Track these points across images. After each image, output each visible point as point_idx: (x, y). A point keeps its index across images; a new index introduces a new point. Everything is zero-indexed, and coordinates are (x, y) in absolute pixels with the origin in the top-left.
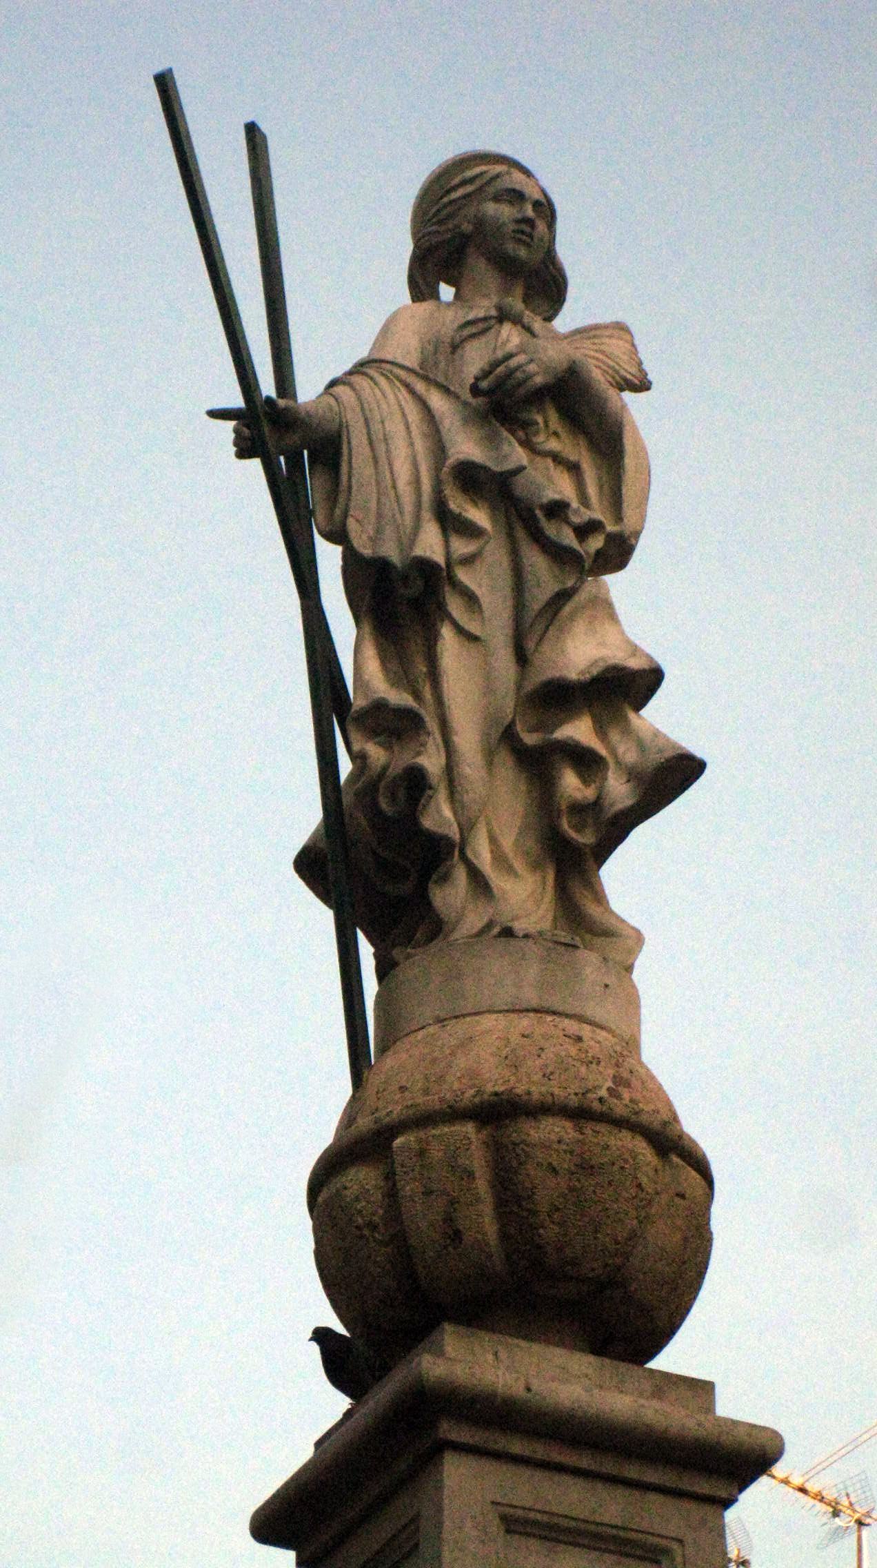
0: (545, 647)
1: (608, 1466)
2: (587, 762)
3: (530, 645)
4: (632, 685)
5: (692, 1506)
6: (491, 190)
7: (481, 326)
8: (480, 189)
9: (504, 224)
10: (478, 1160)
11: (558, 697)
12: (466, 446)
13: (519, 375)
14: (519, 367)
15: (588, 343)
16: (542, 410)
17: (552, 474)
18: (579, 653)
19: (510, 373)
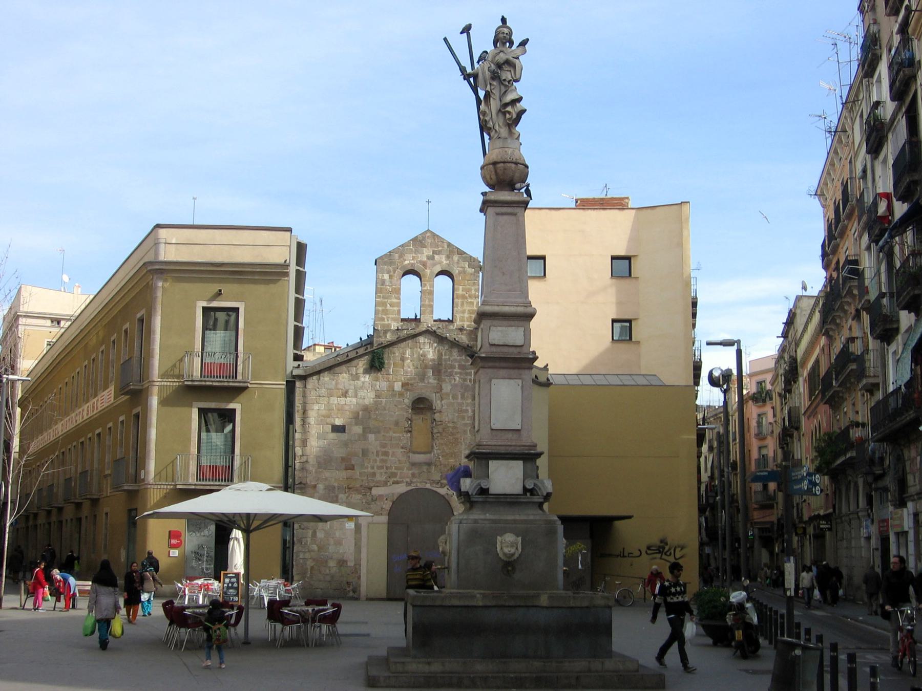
2: (509, 113)
10: (492, 169)
11: (506, 105)
17: (506, 75)
18: (509, 97)
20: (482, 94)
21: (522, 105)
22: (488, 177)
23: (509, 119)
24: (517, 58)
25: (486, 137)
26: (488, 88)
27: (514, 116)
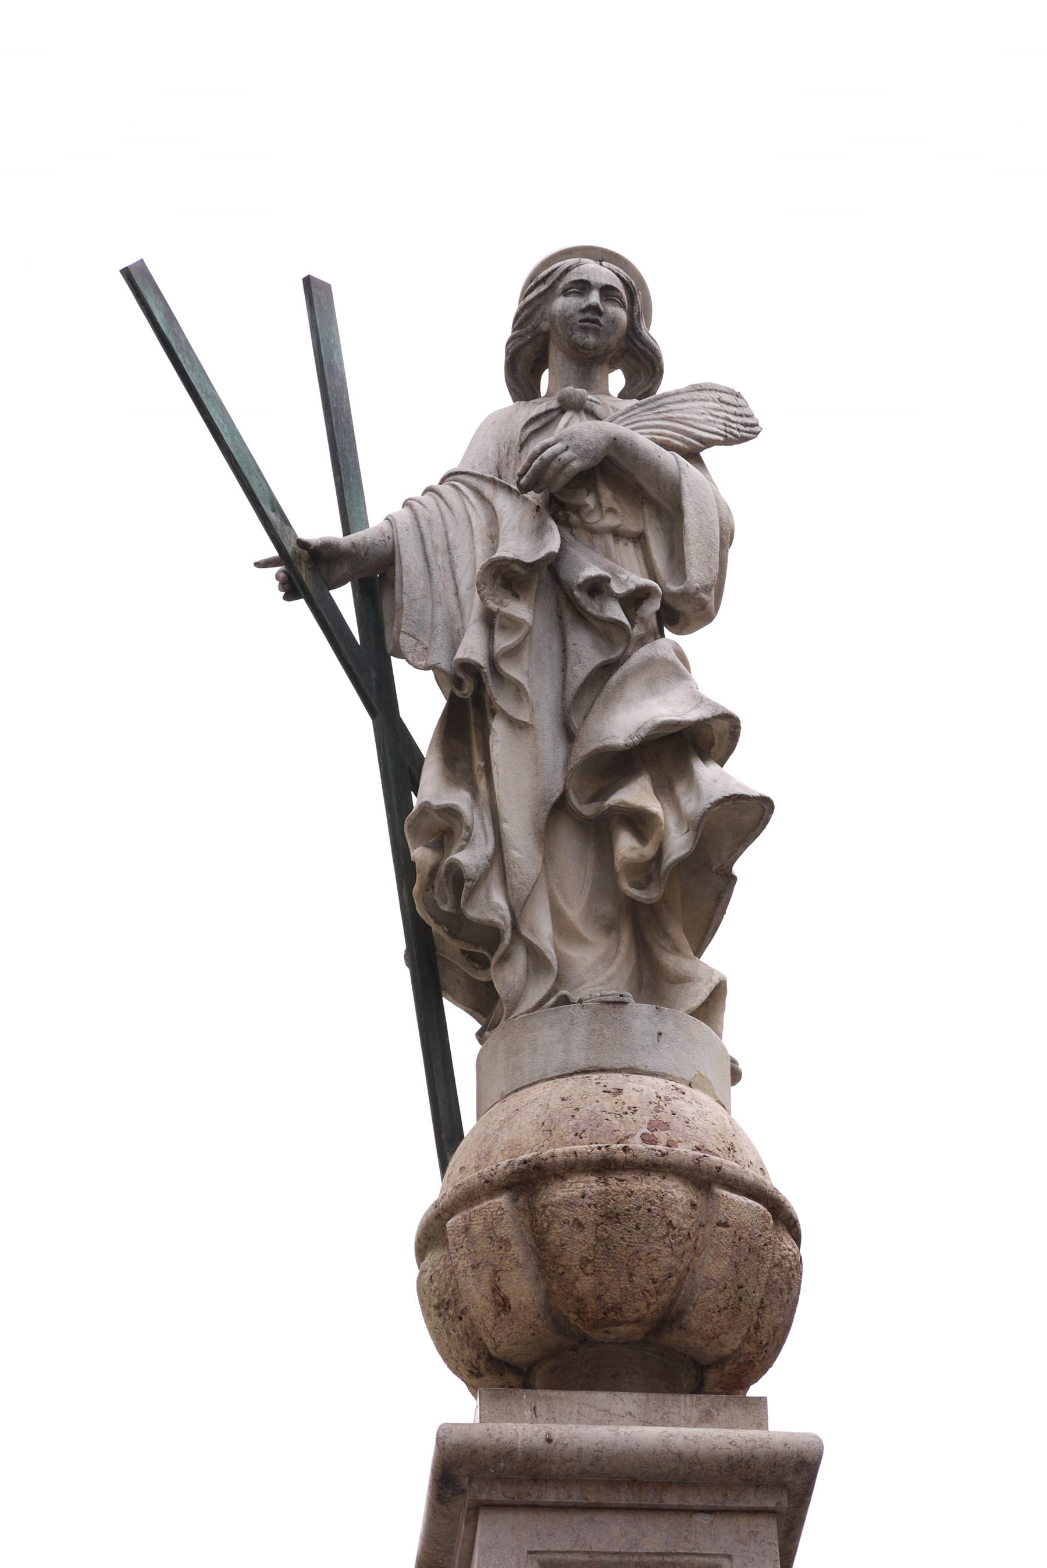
0: (591, 720)
1: (649, 1498)
2: (638, 822)
3: (575, 722)
4: (712, 736)
5: (743, 1521)
6: (561, 286)
7: (544, 420)
8: (553, 285)
9: (572, 316)
12: (519, 545)
13: (555, 464)
14: (555, 456)
15: (650, 415)
16: (593, 489)
18: (630, 717)
19: (546, 464)
20: (421, 701)
21: (742, 772)
22: (476, 1295)
23: (648, 870)
24: (693, 456)
25: (461, 1025)
26: (473, 647)
27: (678, 843)
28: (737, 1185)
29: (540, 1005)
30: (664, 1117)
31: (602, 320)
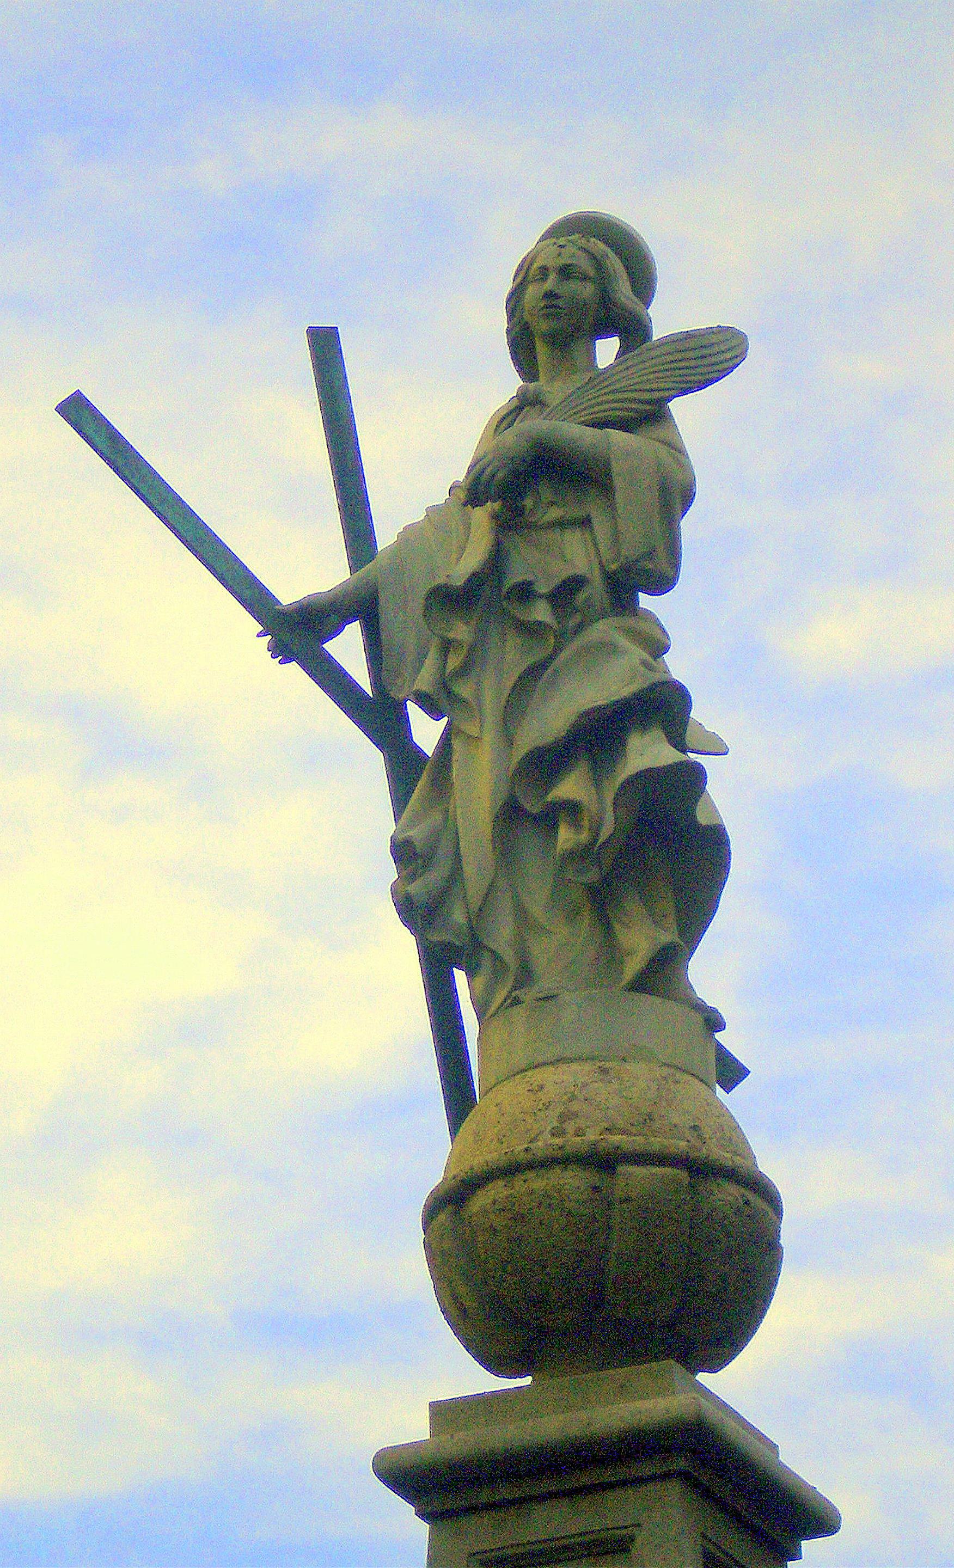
28: (639, 1158)
29: (502, 1004)
30: (575, 1106)
31: (560, 303)
